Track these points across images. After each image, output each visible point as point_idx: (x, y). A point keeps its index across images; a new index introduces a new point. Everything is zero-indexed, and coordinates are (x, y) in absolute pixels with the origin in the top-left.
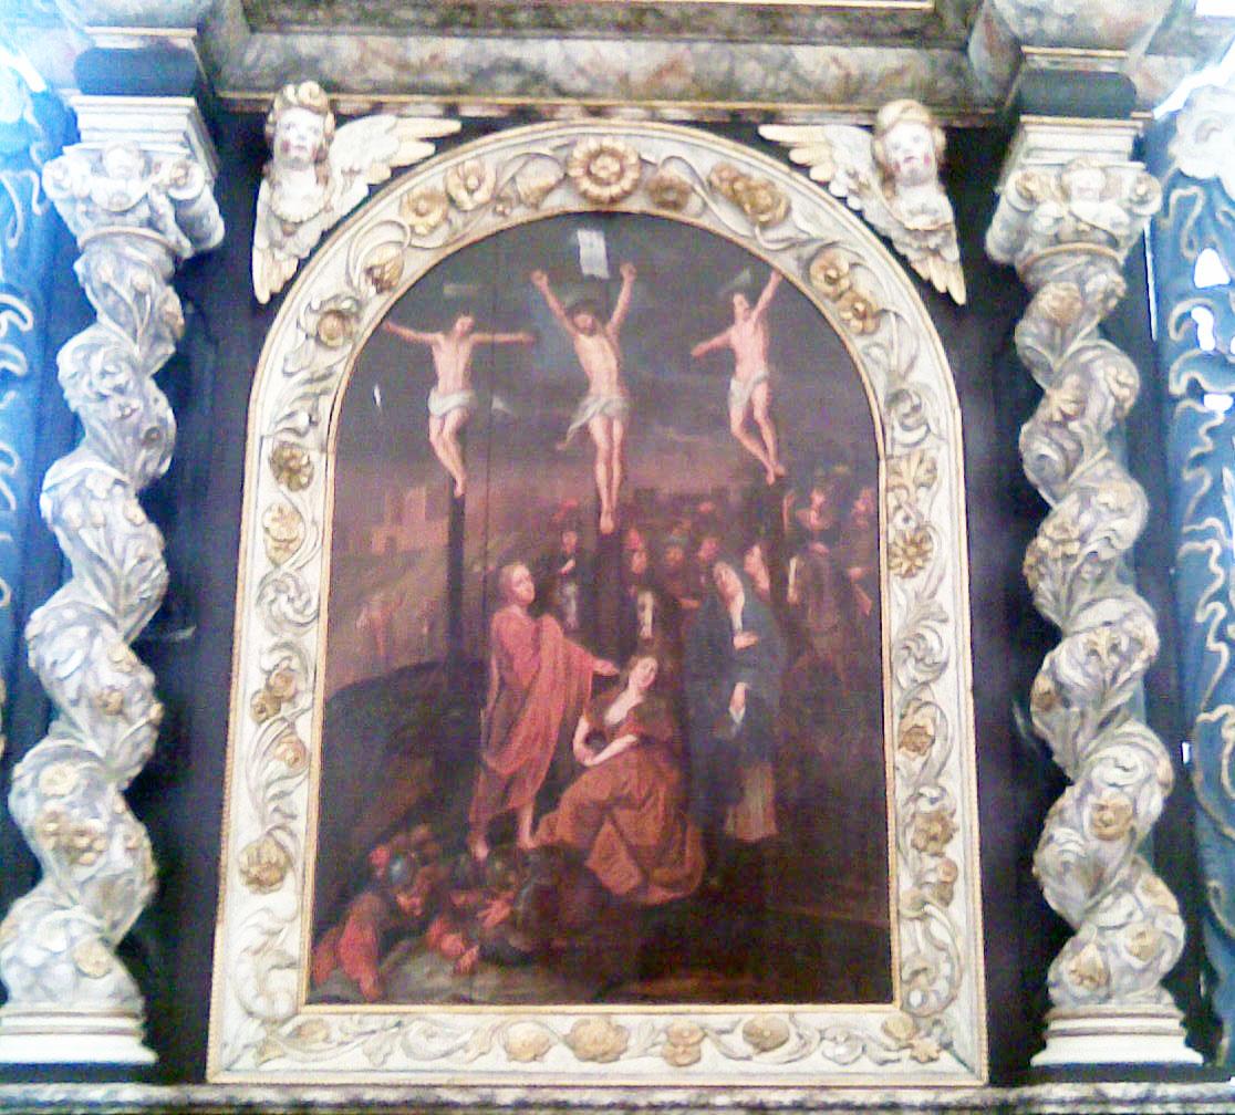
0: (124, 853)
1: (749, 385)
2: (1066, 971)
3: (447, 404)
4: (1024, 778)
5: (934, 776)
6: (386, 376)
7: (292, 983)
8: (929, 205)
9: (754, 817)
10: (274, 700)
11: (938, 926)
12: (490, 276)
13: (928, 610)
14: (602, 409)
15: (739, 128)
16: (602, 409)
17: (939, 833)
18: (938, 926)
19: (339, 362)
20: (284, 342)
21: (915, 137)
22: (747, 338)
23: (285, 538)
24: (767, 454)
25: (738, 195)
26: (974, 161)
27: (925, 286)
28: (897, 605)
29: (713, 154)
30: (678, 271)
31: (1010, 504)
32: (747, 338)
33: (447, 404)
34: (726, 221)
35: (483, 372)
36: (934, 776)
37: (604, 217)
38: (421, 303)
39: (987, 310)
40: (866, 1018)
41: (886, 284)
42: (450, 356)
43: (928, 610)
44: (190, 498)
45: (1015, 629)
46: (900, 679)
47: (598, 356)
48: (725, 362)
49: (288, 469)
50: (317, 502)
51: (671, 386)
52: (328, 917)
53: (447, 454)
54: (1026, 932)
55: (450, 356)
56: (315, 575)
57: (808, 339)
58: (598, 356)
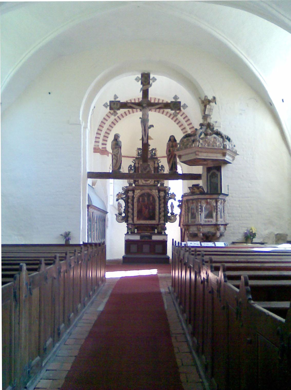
0: (132, 216)
2: (161, 220)
3: (141, 200)
4: (160, 213)
7: (136, 220)
8: (157, 193)
9: (151, 215)
10: (135, 211)
12: (142, 195)
18: (157, 218)
19: (137, 199)
21: (157, 191)
23: (136, 205)
24: (152, 202)
27: (157, 196)
28: (156, 207)
29: (150, 191)
30: (149, 195)
31: (160, 204)
33: (141, 200)
34: (151, 193)
35: (142, 199)
38: (140, 196)
39: (159, 197)
45: (160, 209)
46: (156, 210)
48: (150, 198)
49: (136, 203)
50: (136, 204)
51: (148, 199)
52: (137, 218)
53: (141, 202)
54: (159, 218)
56: (136, 206)
57: (153, 197)
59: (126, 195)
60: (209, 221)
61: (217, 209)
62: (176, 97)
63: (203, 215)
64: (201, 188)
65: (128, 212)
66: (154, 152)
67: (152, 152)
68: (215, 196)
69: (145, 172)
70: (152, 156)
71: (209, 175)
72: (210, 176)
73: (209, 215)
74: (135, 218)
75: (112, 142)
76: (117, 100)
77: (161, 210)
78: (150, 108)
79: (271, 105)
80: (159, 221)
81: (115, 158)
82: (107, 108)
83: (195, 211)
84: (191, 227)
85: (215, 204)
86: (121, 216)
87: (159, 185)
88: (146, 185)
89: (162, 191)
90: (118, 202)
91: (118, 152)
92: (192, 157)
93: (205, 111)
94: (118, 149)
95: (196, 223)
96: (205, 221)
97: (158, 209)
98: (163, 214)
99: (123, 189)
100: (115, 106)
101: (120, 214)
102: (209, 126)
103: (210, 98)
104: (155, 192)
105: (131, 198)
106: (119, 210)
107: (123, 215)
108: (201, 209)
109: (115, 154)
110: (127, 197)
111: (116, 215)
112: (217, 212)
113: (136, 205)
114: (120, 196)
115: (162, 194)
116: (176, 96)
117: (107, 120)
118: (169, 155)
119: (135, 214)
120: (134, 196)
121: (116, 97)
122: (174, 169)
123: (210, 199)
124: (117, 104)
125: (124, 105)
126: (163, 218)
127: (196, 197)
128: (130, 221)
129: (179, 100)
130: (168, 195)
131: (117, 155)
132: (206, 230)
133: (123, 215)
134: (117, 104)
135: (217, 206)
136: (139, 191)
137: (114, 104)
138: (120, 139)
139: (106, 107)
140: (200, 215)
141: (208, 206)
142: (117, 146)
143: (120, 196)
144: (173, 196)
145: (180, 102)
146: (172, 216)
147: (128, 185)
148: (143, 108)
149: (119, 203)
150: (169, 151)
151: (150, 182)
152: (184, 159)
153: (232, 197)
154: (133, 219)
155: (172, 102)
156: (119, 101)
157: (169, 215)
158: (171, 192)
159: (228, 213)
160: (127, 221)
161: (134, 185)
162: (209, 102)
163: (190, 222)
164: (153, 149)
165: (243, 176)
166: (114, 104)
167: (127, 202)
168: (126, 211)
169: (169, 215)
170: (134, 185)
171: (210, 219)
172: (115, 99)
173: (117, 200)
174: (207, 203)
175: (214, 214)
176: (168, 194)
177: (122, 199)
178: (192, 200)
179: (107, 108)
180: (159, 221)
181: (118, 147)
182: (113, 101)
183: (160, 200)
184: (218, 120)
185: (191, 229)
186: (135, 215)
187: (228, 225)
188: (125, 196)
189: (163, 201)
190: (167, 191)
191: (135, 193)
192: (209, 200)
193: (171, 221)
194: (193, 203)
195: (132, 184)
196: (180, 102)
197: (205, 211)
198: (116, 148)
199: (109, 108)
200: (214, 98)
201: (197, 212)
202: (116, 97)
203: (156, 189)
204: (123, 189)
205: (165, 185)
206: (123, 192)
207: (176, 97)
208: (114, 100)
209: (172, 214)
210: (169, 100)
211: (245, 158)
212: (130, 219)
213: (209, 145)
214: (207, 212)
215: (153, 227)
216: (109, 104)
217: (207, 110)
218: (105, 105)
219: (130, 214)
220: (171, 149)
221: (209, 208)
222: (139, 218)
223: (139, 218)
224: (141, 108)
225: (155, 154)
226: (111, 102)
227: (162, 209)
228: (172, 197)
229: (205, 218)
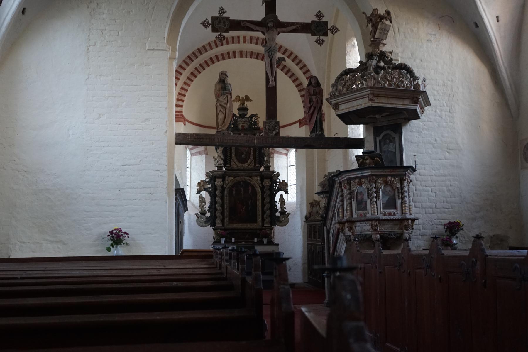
1: (250, 191)
2: (265, 222)
3: (234, 192)
4: (263, 213)
5: (259, 212)
6: (231, 190)
8: (259, 182)
11: (259, 220)
12: (236, 185)
13: (259, 203)
14: (242, 193)
15: (250, 177)
16: (242, 193)
17: (259, 215)
18: (259, 220)
20: (226, 189)
22: (250, 188)
23: (226, 199)
25: (249, 180)
26: (262, 180)
29: (248, 178)
30: (247, 184)
31: (263, 199)
32: (250, 188)
36: (259, 212)
37: (242, 181)
38: (233, 186)
39: (262, 188)
40: (256, 224)
41: (257, 185)
42: (234, 189)
43: (259, 203)
44: (222, 198)
45: (263, 205)
47: (242, 189)
49: (226, 196)
50: (228, 198)
52: (229, 219)
54: (263, 220)
55: (234, 189)
57: (254, 188)
58: (242, 189)
59: (211, 184)
60: (390, 214)
61: (402, 194)
62: (319, 15)
63: (381, 203)
64: (379, 157)
65: (216, 210)
66: (253, 119)
67: (251, 120)
68: (399, 172)
69: (271, 135)
70: (251, 125)
71: (378, 140)
72: (380, 142)
73: (390, 204)
74: (226, 220)
75: (216, 85)
76: (225, 15)
77: (265, 208)
78: (279, 30)
79: (477, 26)
80: (263, 224)
81: (221, 109)
82: (207, 28)
83: (366, 196)
84: (357, 224)
85: (399, 186)
86: (203, 216)
87: (262, 169)
88: (242, 168)
89: (267, 178)
90: (199, 195)
91: (228, 102)
92: (363, 103)
93: (375, 33)
94: (227, 96)
95: (369, 216)
96: (385, 215)
97: (260, 205)
98: (268, 212)
99: (207, 175)
100: (221, 25)
101: (203, 213)
102: (383, 56)
103: (382, 12)
104: (256, 181)
105: (219, 188)
106: (202, 207)
107: (208, 215)
108: (377, 192)
109: (222, 104)
110: (214, 188)
111: (196, 215)
112: (402, 199)
113: (226, 199)
114: (203, 186)
115: (267, 182)
116: (319, 12)
117: (185, 69)
118: (310, 108)
119: (226, 213)
120: (225, 186)
121: (222, 11)
122: (319, 129)
123: (392, 176)
124: (224, 22)
125: (238, 25)
126: (268, 220)
127: (367, 173)
128: (219, 225)
129: (324, 20)
130: (277, 185)
131: (225, 106)
132: (385, 228)
133: (208, 215)
134: (224, 22)
135: (402, 188)
136: (231, 178)
137: (220, 22)
138: (229, 80)
139: (207, 27)
140: (375, 203)
141: (389, 189)
142: (225, 91)
143: (203, 186)
144: (284, 186)
145: (326, 23)
146: (282, 216)
147: (216, 169)
148: (268, 29)
149: (201, 197)
150: (310, 101)
151: (249, 165)
152: (344, 108)
153: (420, 175)
154: (223, 221)
155: (313, 22)
156: (228, 18)
157: (278, 214)
158: (281, 178)
159: (414, 202)
160: (213, 225)
161: (224, 169)
162: (381, 18)
163: (355, 216)
164: (252, 114)
165: (436, 140)
166: (220, 22)
167: (213, 195)
168: (212, 208)
169: (278, 214)
170: (224, 169)
171: (392, 211)
172: (221, 14)
173: (199, 192)
174: (386, 183)
175: (399, 202)
176: (276, 182)
177: (206, 190)
178: (360, 178)
179: (207, 28)
180: (263, 224)
181: (226, 93)
182: (217, 18)
183: (263, 193)
184: (395, 50)
185: (357, 228)
186: (225, 215)
187: (416, 221)
188: (210, 186)
189: (268, 192)
190: (274, 179)
191: (227, 182)
192: (389, 178)
193: (280, 224)
194: (360, 184)
195: (222, 167)
196: (326, 23)
197: (383, 197)
198: (223, 94)
199: (210, 28)
200: (388, 13)
201: (369, 197)
202: (222, 11)
203: (256, 176)
204: (206, 176)
205: (271, 170)
206: (207, 180)
207: (319, 15)
208: (218, 16)
209: (283, 213)
210: (309, 18)
211: (438, 111)
212: (218, 221)
213: (390, 85)
214: (386, 199)
215: (254, 233)
216: (210, 22)
217: (378, 31)
218: (205, 24)
219: (218, 214)
220: (314, 98)
221: (390, 191)
222: (231, 221)
223: (231, 221)
224: (264, 30)
225: (255, 122)
226: (213, 18)
227: (268, 206)
228: (282, 186)
229: (383, 209)
